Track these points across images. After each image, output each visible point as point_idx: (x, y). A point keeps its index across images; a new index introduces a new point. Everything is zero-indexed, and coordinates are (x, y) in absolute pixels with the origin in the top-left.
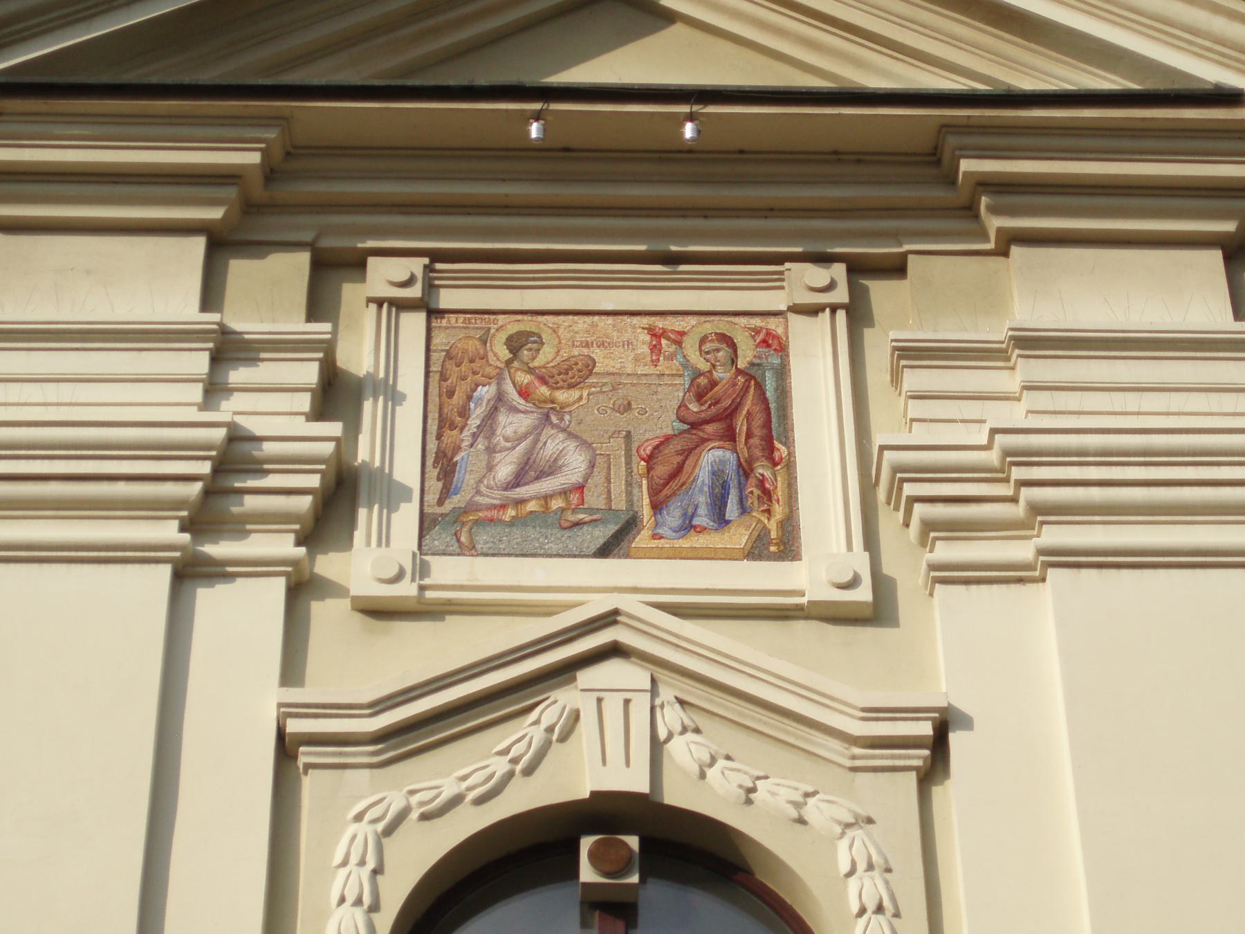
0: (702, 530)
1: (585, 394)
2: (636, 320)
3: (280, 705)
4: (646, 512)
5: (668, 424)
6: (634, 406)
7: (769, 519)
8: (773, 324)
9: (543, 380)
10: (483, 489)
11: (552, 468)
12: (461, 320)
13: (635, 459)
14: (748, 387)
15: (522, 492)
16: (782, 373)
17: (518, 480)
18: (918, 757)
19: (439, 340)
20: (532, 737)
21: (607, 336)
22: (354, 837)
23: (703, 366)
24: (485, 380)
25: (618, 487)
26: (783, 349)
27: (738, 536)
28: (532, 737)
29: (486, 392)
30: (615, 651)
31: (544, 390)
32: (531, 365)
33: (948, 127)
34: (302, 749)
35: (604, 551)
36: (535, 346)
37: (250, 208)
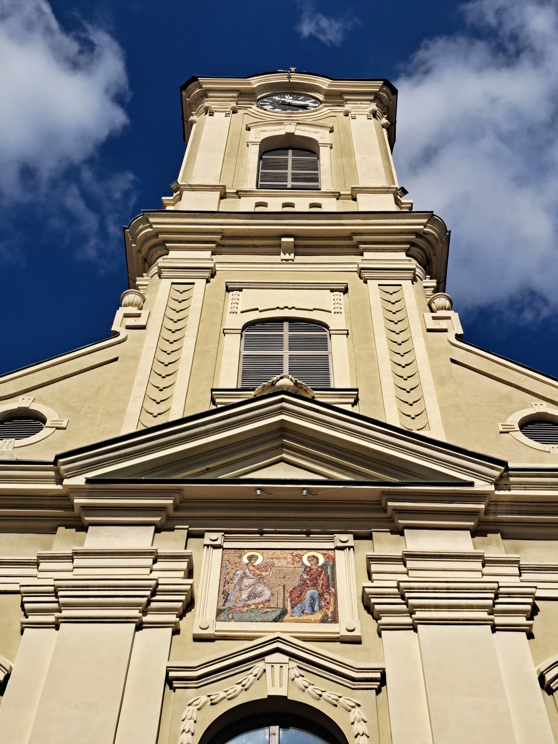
0: (307, 614)
1: (271, 573)
2: (288, 551)
3: (167, 667)
4: (289, 608)
5: (297, 582)
6: (286, 576)
7: (328, 611)
8: (331, 553)
9: (258, 569)
10: (237, 601)
11: (260, 595)
12: (233, 552)
13: (286, 592)
14: (322, 571)
15: (250, 602)
16: (333, 567)
17: (249, 598)
18: (376, 685)
19: (226, 557)
20: (249, 678)
21: (278, 556)
22: (189, 711)
23: (309, 565)
24: (240, 569)
25: (281, 601)
26: (334, 560)
27: (319, 616)
28: (249, 678)
29: (240, 573)
30: (277, 650)
31: (258, 572)
32: (254, 564)
33: (384, 493)
34: (174, 682)
35: (275, 621)
36: (256, 559)
37: (169, 518)
